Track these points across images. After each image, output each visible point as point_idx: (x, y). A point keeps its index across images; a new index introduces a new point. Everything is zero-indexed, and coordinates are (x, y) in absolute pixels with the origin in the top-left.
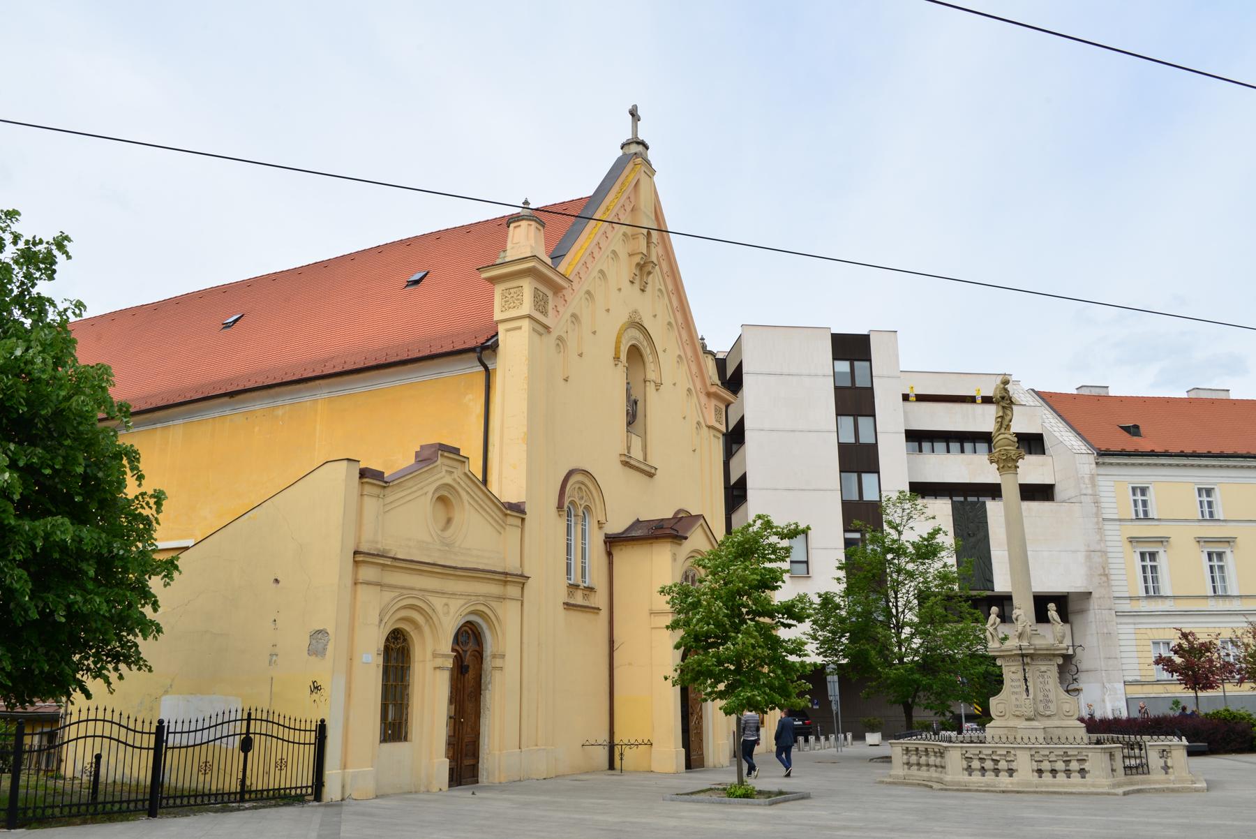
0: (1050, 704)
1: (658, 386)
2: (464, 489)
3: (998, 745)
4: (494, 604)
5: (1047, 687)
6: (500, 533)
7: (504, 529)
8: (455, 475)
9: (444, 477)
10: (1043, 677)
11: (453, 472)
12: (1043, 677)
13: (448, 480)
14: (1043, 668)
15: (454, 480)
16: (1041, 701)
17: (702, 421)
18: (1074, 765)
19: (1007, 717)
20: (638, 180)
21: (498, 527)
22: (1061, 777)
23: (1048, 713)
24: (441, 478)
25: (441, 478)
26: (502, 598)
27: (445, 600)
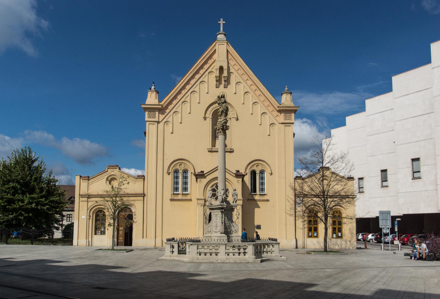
0: (217, 227)
5: (217, 221)
7: (136, 182)
9: (111, 173)
10: (216, 217)
11: (114, 171)
12: (216, 217)
13: (113, 173)
14: (216, 213)
15: (115, 173)
16: (214, 226)
17: (275, 122)
18: (242, 250)
19: (211, 232)
21: (134, 182)
22: (237, 255)
23: (216, 231)
24: (110, 173)
25: (110, 173)
26: (134, 200)
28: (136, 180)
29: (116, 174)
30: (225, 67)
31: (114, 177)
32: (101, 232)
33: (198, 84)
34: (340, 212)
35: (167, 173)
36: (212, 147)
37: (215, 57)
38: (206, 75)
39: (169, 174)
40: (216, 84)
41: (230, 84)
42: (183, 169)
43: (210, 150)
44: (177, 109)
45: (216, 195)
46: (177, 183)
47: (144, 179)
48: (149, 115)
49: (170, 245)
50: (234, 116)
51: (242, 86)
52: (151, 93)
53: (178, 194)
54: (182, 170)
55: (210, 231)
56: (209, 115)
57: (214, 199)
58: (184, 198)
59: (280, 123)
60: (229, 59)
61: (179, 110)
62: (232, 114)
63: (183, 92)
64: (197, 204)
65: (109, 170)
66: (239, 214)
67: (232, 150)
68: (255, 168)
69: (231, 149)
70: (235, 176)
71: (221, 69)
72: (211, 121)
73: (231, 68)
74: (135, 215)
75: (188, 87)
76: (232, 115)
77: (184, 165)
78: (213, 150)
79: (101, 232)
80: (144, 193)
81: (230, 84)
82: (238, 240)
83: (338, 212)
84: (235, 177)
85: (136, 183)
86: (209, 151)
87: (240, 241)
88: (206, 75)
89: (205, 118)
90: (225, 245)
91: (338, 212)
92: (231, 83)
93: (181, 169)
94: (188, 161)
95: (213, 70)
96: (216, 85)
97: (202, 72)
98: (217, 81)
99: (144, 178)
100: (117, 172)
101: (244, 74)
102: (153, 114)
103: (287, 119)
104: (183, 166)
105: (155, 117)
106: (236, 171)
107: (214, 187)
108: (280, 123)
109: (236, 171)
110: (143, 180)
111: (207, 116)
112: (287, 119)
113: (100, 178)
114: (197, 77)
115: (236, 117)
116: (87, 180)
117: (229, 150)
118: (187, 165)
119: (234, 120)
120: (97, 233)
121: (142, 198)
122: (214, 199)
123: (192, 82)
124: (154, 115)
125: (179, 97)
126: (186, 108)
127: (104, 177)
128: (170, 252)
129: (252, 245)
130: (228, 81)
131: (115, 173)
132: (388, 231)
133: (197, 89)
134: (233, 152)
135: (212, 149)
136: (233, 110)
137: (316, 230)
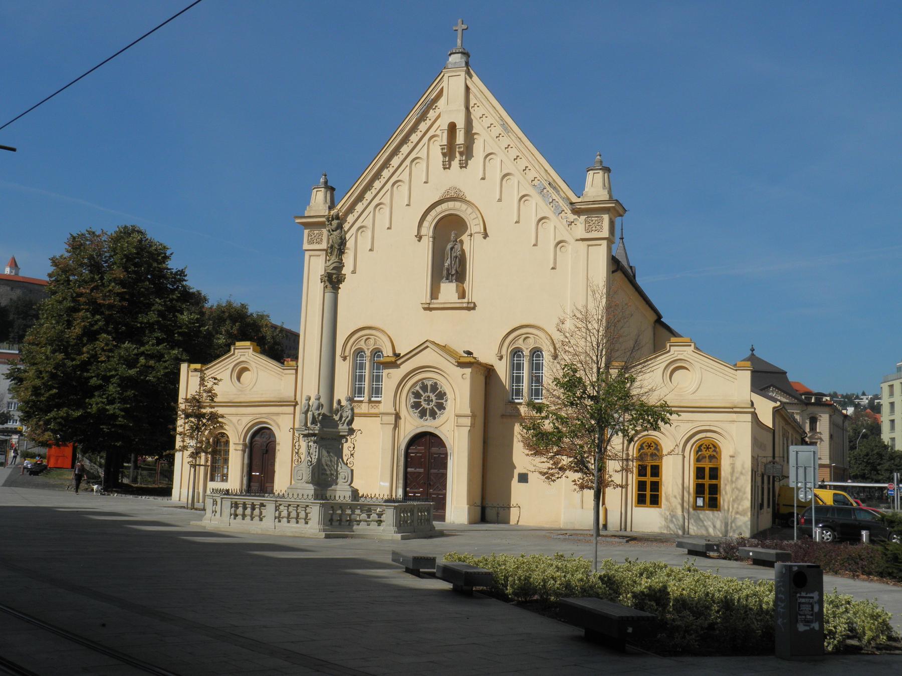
1: (486, 235)
2: (253, 361)
3: (296, 500)
4: (274, 418)
6: (281, 380)
8: (247, 355)
11: (245, 355)
13: (242, 359)
15: (246, 358)
20: (442, 90)
24: (238, 359)
25: (238, 359)
27: (238, 418)
28: (283, 373)
29: (249, 359)
30: (461, 124)
31: (245, 366)
32: (223, 475)
33: (407, 166)
34: (714, 446)
35: (342, 357)
36: (432, 299)
37: (441, 103)
38: (425, 144)
39: (345, 358)
40: (443, 162)
41: (473, 157)
42: (371, 348)
43: (426, 306)
44: (364, 221)
45: (422, 405)
46: (361, 378)
47: (297, 370)
48: (310, 238)
49: (212, 500)
50: (478, 230)
51: (499, 160)
52: (317, 191)
53: (361, 402)
54: (370, 350)
55: (300, 478)
56: (428, 230)
57: (416, 413)
58: (373, 411)
59: (577, 240)
60: (471, 104)
61: (368, 223)
62: (475, 225)
63: (377, 185)
64: (381, 424)
65: (236, 351)
66: (354, 448)
67: (472, 305)
68: (520, 344)
69: (468, 303)
70: (456, 364)
71: (452, 128)
72: (431, 243)
73: (475, 124)
74: (279, 444)
75: (386, 173)
76: (474, 227)
77: (375, 339)
78: (431, 306)
79: (223, 475)
80: (295, 399)
81: (473, 157)
82: (344, 497)
83: (711, 446)
84: (457, 366)
85: (283, 378)
86: (425, 309)
87: (310, 497)
88: (425, 144)
89: (419, 237)
90: (274, 502)
91: (711, 448)
92: (474, 155)
93: (369, 347)
94: (383, 331)
95: (439, 132)
96: (443, 165)
97: (414, 138)
98: (444, 155)
99: (295, 368)
100: (249, 355)
101: (503, 134)
102: (318, 235)
103: (592, 229)
104: (372, 341)
105: (322, 240)
106: (464, 352)
107: (418, 388)
108: (577, 240)
109: (464, 352)
110: (294, 371)
111: (424, 231)
112: (592, 229)
113: (219, 367)
114: (405, 149)
115: (482, 231)
116: (199, 373)
117: (465, 305)
118: (379, 340)
119: (479, 238)
120: (216, 477)
121: (292, 408)
122: (416, 413)
123: (395, 162)
124: (320, 237)
125: (368, 196)
126: (383, 217)
127: (227, 367)
128: (231, 515)
129: (393, 508)
130: (468, 152)
131: (246, 358)
132: (810, 497)
133: (405, 176)
134: (474, 308)
135: (429, 304)
136: (476, 215)
137: (656, 486)
